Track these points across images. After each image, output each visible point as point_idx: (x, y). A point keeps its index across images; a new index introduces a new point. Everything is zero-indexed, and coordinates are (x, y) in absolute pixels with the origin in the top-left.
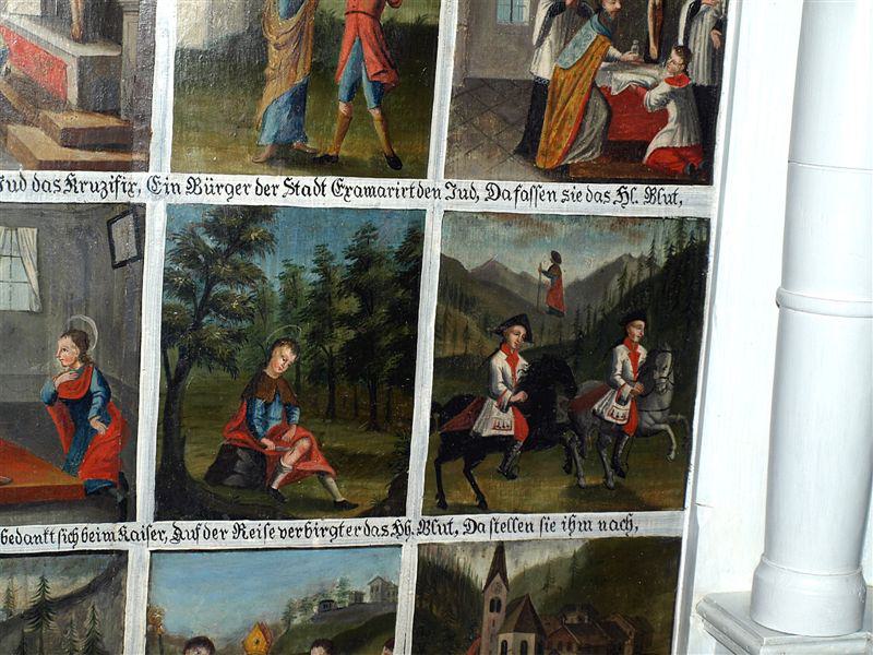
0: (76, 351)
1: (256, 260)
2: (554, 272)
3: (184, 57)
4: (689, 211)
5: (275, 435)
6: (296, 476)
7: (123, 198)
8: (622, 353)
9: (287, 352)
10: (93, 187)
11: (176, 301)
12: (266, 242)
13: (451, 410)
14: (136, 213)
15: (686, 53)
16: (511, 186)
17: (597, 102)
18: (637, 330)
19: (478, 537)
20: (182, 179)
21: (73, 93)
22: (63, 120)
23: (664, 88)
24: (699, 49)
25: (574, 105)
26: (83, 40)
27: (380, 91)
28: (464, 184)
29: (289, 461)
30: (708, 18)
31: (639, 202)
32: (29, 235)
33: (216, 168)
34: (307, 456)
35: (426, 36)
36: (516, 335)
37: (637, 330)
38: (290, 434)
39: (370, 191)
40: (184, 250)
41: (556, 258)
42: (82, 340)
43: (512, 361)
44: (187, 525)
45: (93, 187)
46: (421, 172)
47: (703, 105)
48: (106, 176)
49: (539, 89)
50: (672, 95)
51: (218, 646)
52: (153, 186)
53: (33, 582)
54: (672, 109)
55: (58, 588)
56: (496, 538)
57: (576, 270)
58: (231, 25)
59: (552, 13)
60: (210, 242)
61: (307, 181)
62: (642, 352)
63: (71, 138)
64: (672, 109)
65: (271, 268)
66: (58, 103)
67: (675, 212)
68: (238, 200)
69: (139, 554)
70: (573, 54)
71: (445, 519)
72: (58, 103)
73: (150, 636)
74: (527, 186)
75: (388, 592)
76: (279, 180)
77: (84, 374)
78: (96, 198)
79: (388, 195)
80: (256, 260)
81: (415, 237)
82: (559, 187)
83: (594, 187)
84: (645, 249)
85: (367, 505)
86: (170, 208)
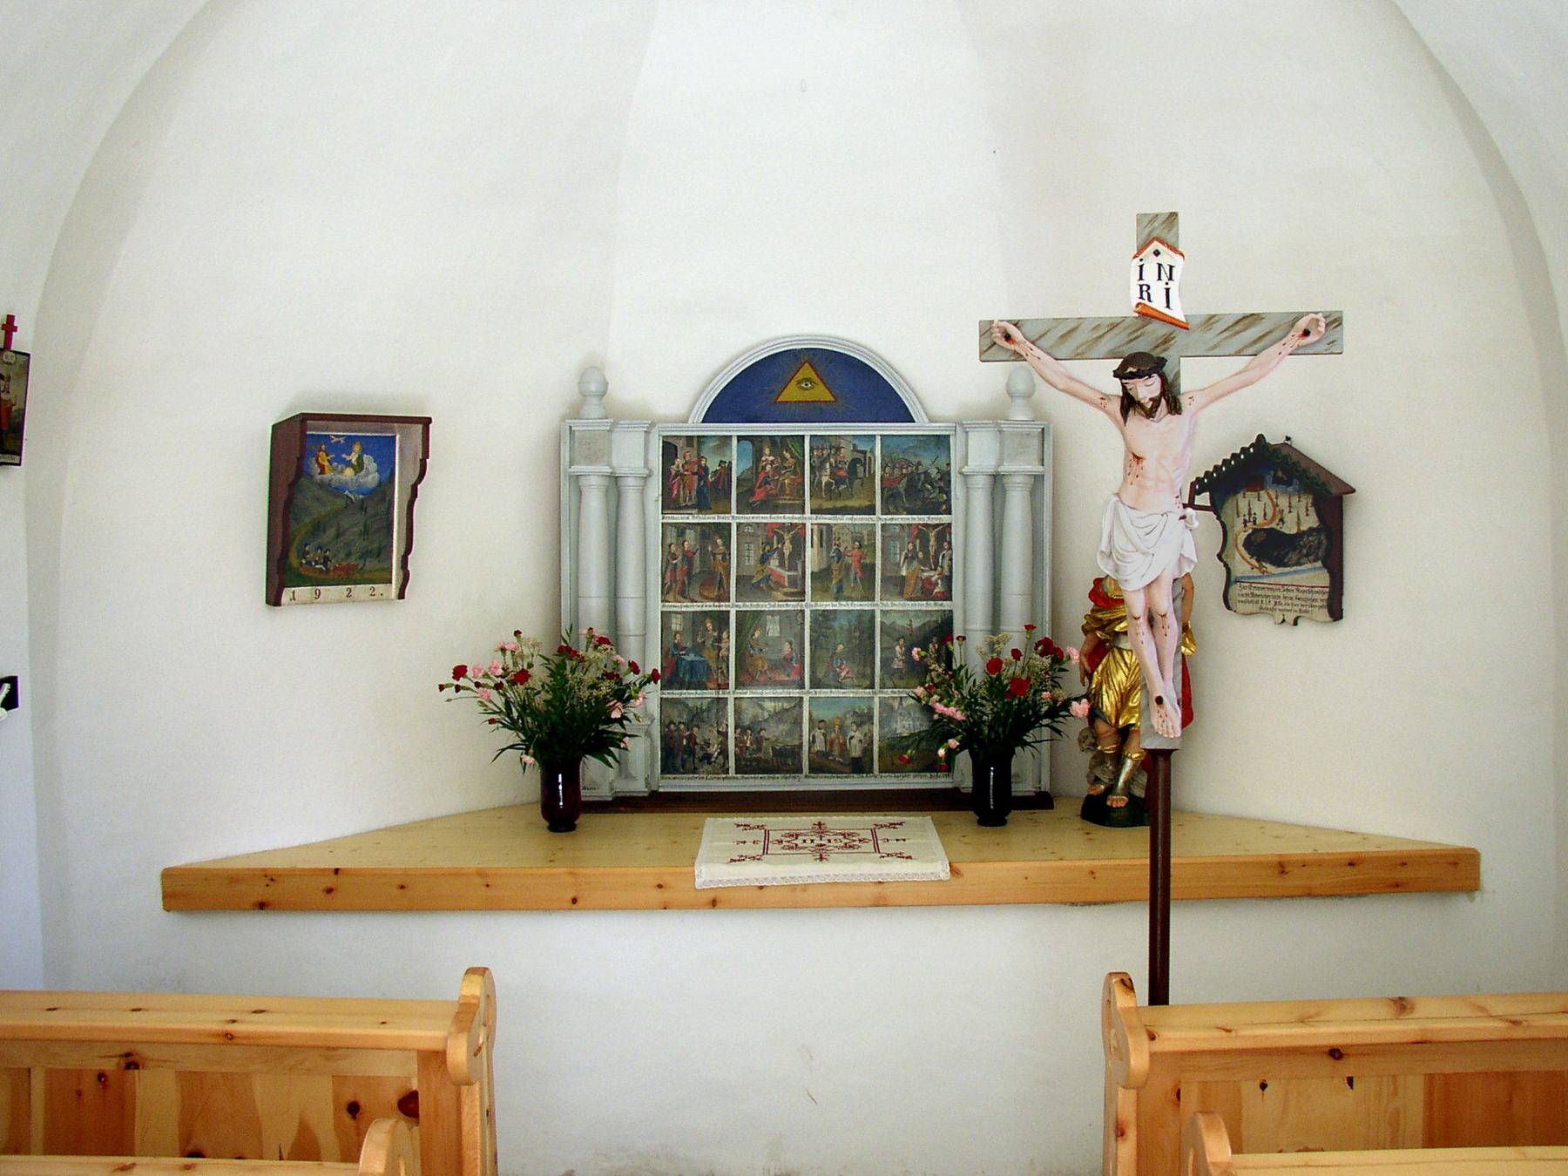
0: (789, 646)
1: (832, 623)
2: (910, 625)
3: (812, 573)
4: (947, 608)
5: (840, 667)
6: (845, 678)
7: (799, 608)
8: (931, 646)
9: (841, 646)
10: (793, 605)
11: (813, 634)
12: (834, 619)
13: (886, 663)
14: (802, 612)
15: (942, 567)
16: (896, 603)
17: (919, 581)
18: (934, 640)
19: (894, 695)
20: (813, 603)
21: (786, 584)
22: (785, 590)
23: (937, 576)
24: (946, 567)
25: (912, 582)
26: (789, 570)
27: (862, 580)
28: (885, 602)
29: (843, 674)
30: (947, 558)
31: (931, 606)
32: (777, 618)
33: (822, 601)
34: (848, 673)
35: (873, 566)
36: (902, 641)
37: (934, 640)
38: (843, 667)
39: (861, 605)
40: (814, 621)
41: (911, 621)
42: (791, 643)
43: (901, 648)
44: (818, 690)
45: (793, 605)
46: (874, 600)
47: (948, 580)
48: (794, 603)
49: (903, 577)
50: (938, 578)
51: (827, 722)
52: (806, 605)
53: (780, 704)
54: (939, 582)
55: (786, 705)
56: (901, 695)
57: (916, 624)
58: (824, 566)
59: (905, 558)
60: (820, 618)
61: (844, 603)
62: (937, 646)
63: (786, 594)
64: (939, 582)
65: (836, 625)
66: (784, 587)
67: (942, 608)
68: (828, 608)
69: (806, 698)
70: (912, 568)
71: (885, 690)
72: (784, 587)
73: (810, 719)
74: (902, 603)
75: (871, 710)
76: (837, 603)
77: (791, 652)
78: (793, 609)
79: (866, 606)
80: (832, 623)
81: (873, 617)
82: (910, 603)
83: (920, 602)
84: (935, 619)
85: (865, 686)
86: (811, 611)
